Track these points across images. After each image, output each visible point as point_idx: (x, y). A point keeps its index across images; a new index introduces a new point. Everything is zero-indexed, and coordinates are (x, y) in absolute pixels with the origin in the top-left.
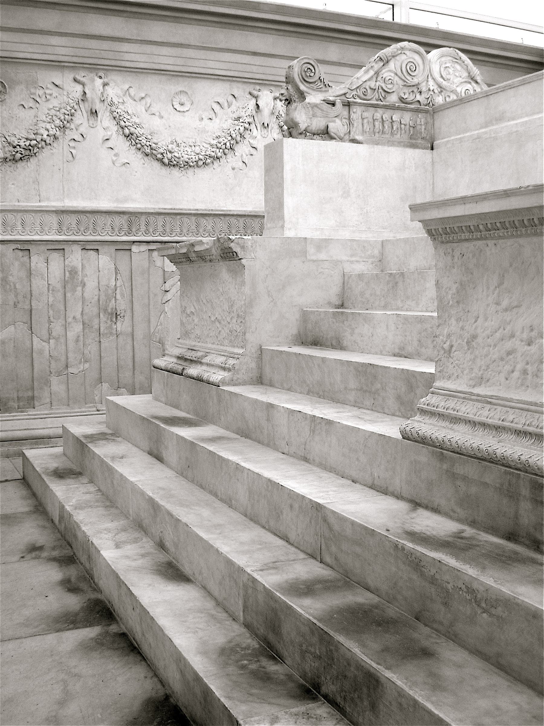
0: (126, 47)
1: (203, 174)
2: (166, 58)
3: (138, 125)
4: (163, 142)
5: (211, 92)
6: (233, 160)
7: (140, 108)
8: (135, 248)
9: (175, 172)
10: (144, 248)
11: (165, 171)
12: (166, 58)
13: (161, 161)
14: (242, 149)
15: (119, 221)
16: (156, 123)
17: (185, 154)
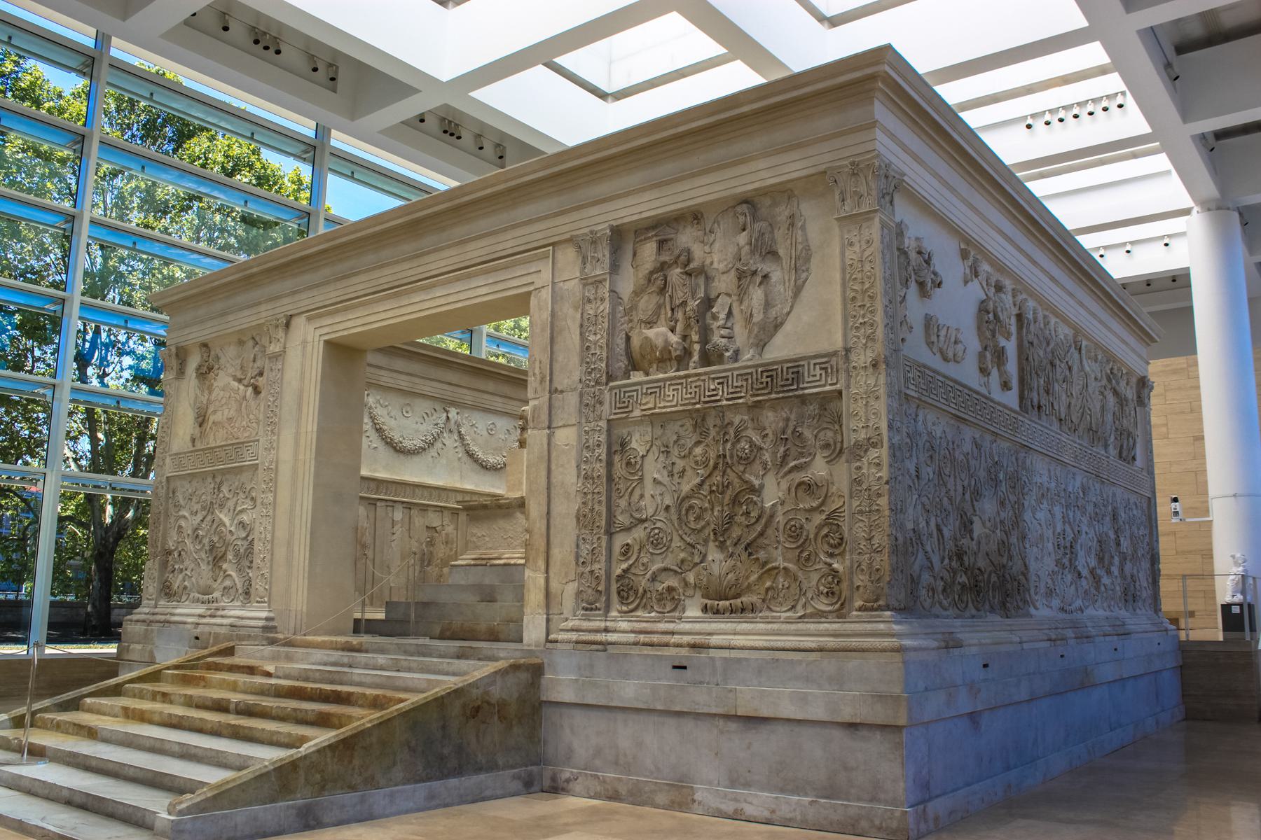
0: (382, 372)
1: (416, 459)
2: (403, 382)
3: (384, 423)
4: (397, 438)
5: (423, 406)
6: (433, 452)
7: (385, 412)
8: (379, 504)
9: (402, 456)
10: (383, 504)
11: (396, 455)
12: (403, 382)
13: (395, 448)
14: (438, 445)
15: (373, 485)
16: (393, 423)
17: (408, 444)
